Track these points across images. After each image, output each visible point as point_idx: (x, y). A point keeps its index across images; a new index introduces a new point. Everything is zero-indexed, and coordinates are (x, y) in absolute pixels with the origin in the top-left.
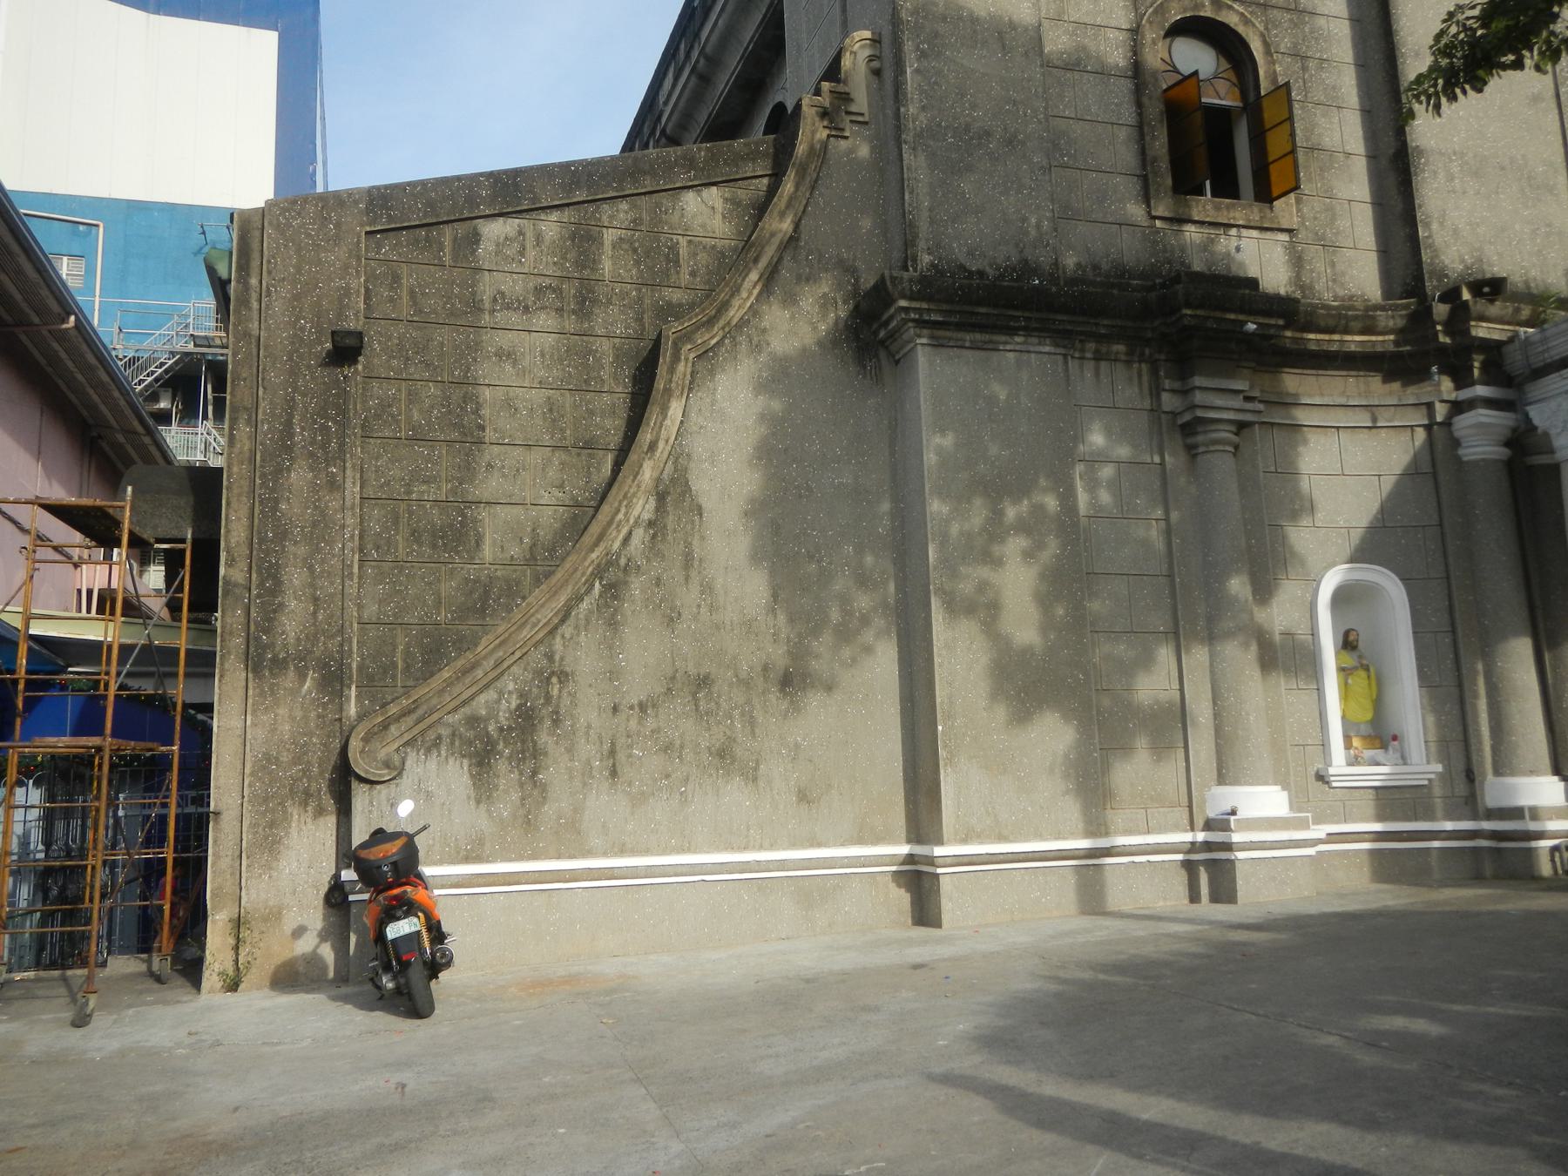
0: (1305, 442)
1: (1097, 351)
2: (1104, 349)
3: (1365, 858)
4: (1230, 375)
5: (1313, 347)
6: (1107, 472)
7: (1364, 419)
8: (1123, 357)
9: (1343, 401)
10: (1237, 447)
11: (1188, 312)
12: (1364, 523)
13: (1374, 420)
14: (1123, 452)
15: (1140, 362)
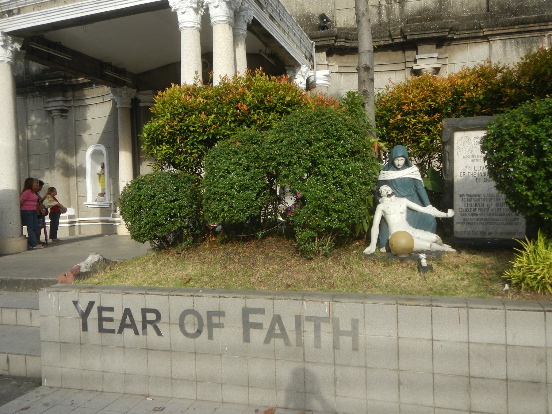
0: (89, 109)
1: (32, 95)
2: (33, 94)
3: (100, 226)
4: (58, 96)
5: (81, 82)
6: (35, 127)
7: (100, 100)
8: (39, 95)
9: (95, 96)
10: (61, 116)
11: (35, 83)
12: (101, 132)
13: (103, 100)
14: (39, 120)
15: (44, 95)
